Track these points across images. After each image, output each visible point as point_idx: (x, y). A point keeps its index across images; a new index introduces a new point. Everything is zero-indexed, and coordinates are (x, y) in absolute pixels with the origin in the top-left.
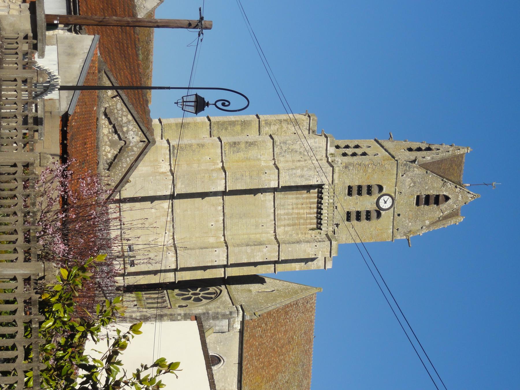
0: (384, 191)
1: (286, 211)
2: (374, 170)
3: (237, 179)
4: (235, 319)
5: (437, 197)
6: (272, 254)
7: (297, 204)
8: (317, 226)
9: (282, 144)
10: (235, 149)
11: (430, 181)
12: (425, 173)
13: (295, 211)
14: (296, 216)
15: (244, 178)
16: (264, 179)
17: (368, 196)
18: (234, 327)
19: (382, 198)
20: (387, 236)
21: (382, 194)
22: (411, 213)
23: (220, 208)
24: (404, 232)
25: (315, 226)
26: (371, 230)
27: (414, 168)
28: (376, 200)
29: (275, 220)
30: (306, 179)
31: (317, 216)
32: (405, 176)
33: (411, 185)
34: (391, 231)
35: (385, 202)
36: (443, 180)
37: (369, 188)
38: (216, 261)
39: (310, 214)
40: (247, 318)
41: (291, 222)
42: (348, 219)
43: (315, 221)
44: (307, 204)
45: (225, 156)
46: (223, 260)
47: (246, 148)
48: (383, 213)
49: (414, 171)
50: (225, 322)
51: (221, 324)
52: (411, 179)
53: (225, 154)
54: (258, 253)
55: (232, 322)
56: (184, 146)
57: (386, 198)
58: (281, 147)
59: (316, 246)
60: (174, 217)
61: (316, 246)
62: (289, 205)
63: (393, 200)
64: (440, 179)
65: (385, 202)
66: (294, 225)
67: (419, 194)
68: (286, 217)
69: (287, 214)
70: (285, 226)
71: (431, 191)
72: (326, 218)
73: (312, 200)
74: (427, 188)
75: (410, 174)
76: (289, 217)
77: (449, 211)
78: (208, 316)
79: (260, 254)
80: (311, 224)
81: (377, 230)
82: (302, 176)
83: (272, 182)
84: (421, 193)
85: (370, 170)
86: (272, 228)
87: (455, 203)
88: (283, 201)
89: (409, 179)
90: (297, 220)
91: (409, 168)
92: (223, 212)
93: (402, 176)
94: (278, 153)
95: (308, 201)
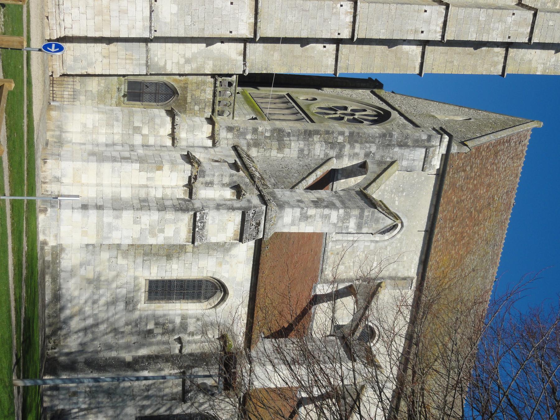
4: (435, 150)
6: (521, 30)
18: (432, 163)
38: (422, 32)
46: (436, 32)
50: (420, 153)
51: (411, 156)
54: (497, 25)
55: (430, 154)
78: (390, 141)
79: (500, 26)
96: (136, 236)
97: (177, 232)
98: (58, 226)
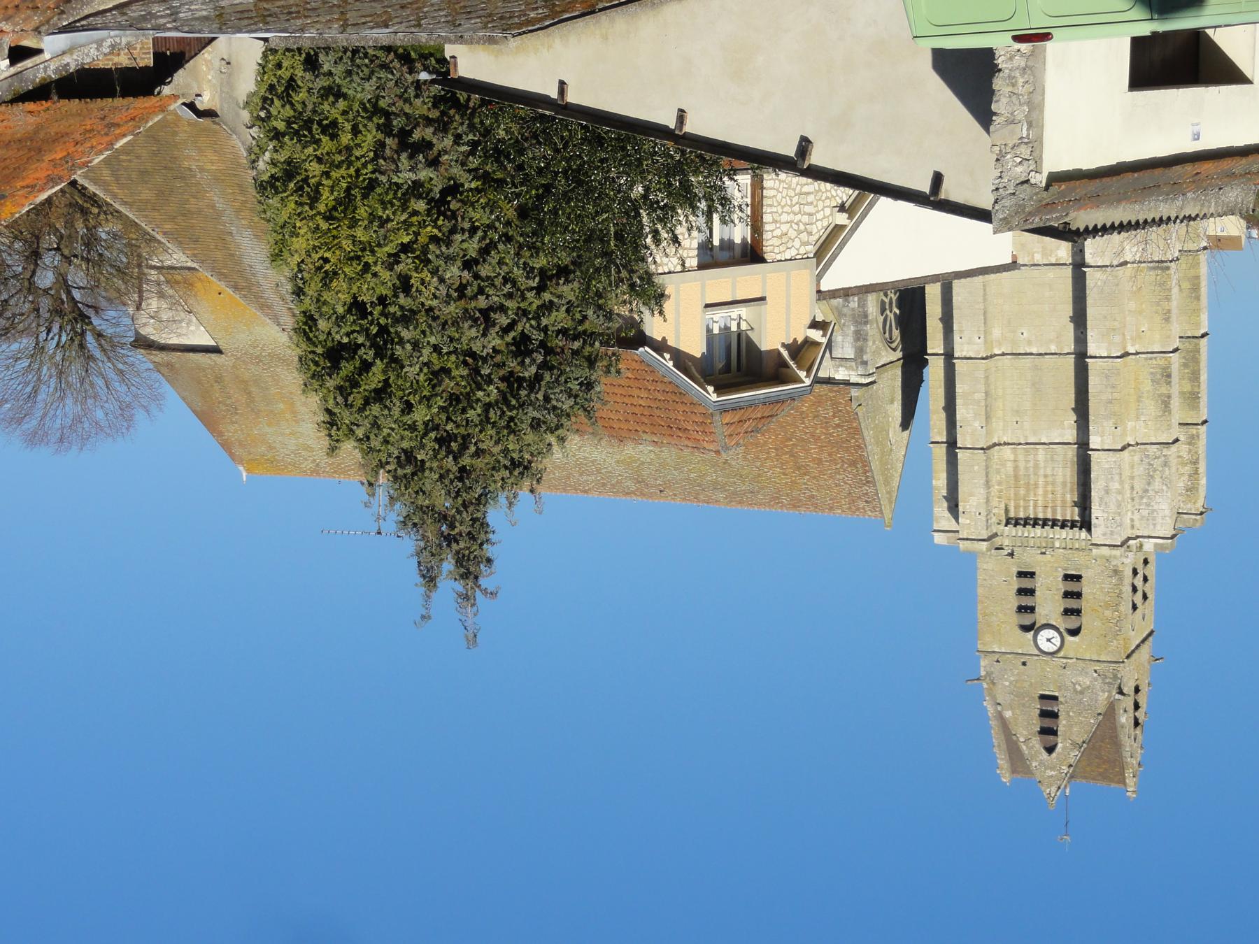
0: (1069, 638)
1: (1042, 464)
2: (1108, 620)
3: (1107, 377)
4: (853, 370)
5: (1054, 733)
6: (968, 438)
7: (1053, 483)
8: (1012, 518)
9: (1163, 458)
10: (1159, 376)
11: (1083, 719)
12: (1099, 712)
13: (1041, 481)
14: (1032, 482)
15: (1110, 390)
16: (1105, 424)
17: (1062, 610)
18: (840, 369)
19: (1056, 634)
21: (1065, 634)
22: (1026, 685)
23: (1053, 349)
24: (992, 673)
25: (1012, 515)
26: (1000, 615)
27: (1109, 691)
28: (1054, 624)
29: (1027, 444)
30: (1101, 499)
31: (1031, 519)
32: (1095, 675)
33: (1077, 686)
34: (996, 650)
35: (1049, 640)
36: (1084, 742)
37: (1077, 612)
39: (1035, 506)
40: (854, 392)
41: (1021, 473)
42: (1021, 574)
43: (1022, 515)
44: (1053, 501)
45: (1146, 359)
46: (962, 351)
47: (1160, 395)
48: (1030, 635)
49: (1103, 691)
50: (849, 353)
51: (847, 345)
52: (1088, 687)
53: (1151, 359)
54: (971, 411)
55: (849, 364)
56: (1168, 287)
57: (1057, 641)
58: (1158, 458)
59: (980, 514)
60: (1039, 267)
61: (980, 514)
62: (1053, 469)
63: (1052, 654)
64: (1085, 737)
65: (1049, 640)
66: (1016, 477)
67: (1061, 699)
68: (1031, 464)
69: (1036, 466)
70: (1015, 461)
71: (1064, 722)
72: (1026, 535)
73: (1059, 510)
74: (1071, 714)
75: (1098, 684)
76: (1032, 469)
77: (1026, 752)
78: (861, 323)
80: (1017, 507)
81: (998, 625)
82: (1107, 491)
83: (1100, 439)
84: (1062, 703)
85: (1108, 613)
86: (1011, 439)
87: (1041, 763)
88: (1060, 458)
89: (1088, 683)
90: (1025, 484)
91: (1109, 683)
92: (1046, 354)
93: (1095, 671)
94: (1148, 451)
95: (1059, 503)
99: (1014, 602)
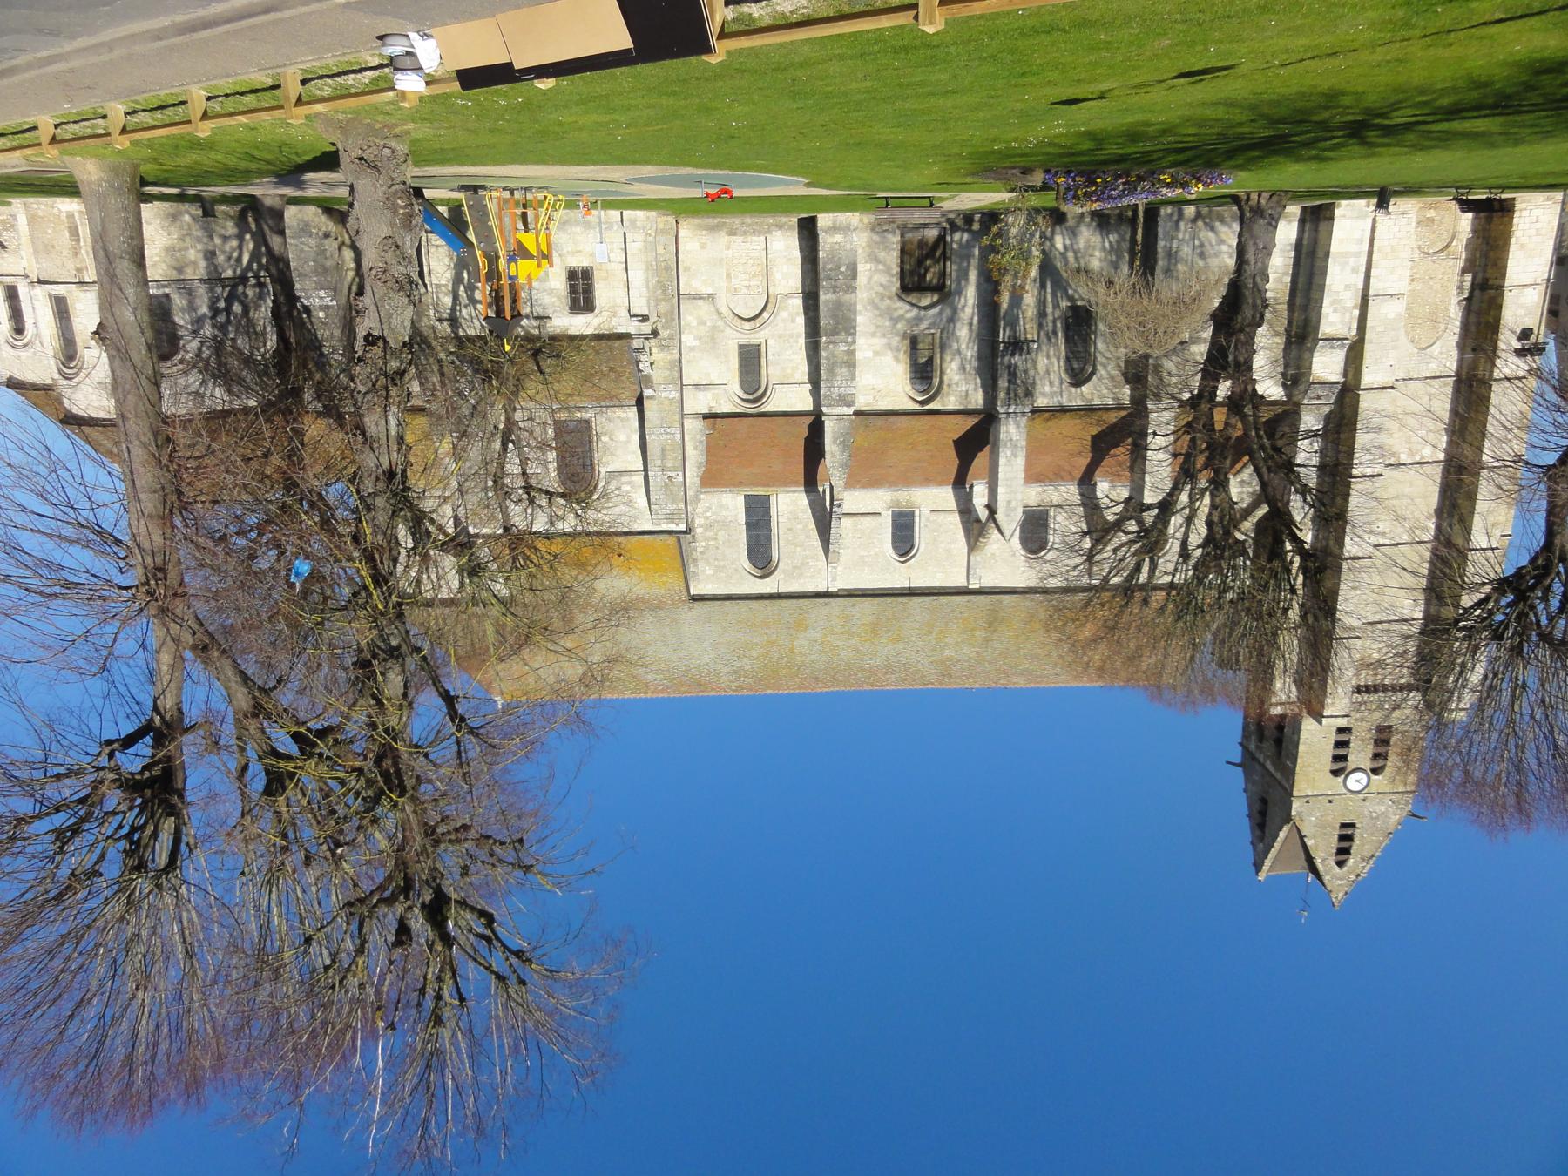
20: (1301, 787)
57: (1365, 781)
63: (1359, 792)
96: (1334, 288)
97: (1332, 324)
98: (1352, 218)
99: (1329, 751)
